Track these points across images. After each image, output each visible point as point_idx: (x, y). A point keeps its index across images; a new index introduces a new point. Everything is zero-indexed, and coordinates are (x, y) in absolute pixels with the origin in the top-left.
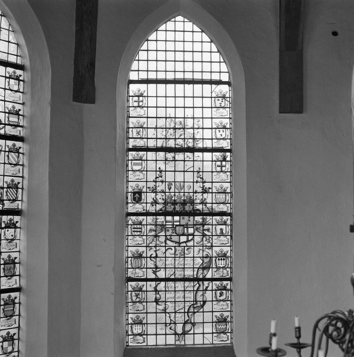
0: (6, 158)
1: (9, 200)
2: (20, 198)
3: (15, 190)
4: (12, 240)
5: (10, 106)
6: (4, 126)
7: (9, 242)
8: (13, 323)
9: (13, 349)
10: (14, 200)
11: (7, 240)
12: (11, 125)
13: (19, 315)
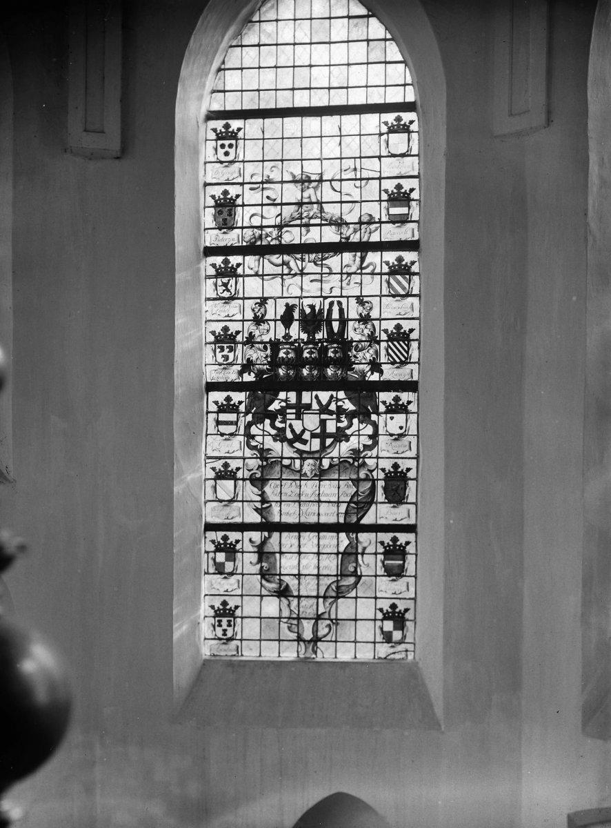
0: (385, 285)
1: (393, 363)
2: (415, 357)
3: (405, 344)
4: (401, 436)
5: (390, 185)
6: (379, 225)
7: (395, 439)
8: (404, 588)
9: (404, 637)
10: (403, 363)
11: (391, 435)
12: (394, 223)
13: (415, 577)
